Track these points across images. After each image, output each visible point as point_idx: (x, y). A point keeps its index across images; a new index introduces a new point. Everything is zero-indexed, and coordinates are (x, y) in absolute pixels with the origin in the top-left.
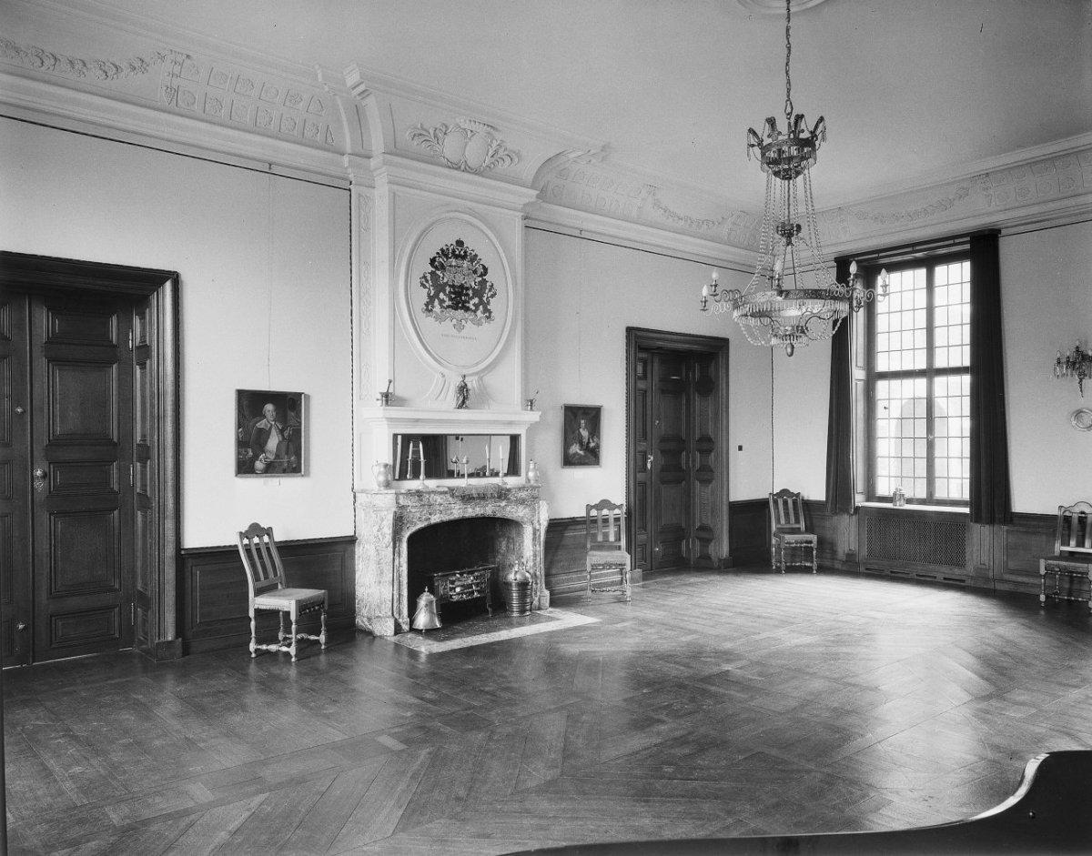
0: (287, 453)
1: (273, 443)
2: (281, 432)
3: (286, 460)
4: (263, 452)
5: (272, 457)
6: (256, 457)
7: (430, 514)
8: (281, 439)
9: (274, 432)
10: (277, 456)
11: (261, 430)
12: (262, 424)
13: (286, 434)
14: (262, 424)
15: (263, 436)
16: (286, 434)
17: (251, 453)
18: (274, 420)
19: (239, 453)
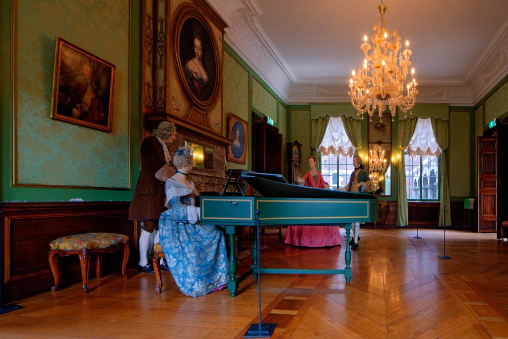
2: (96, 91)
6: (73, 105)
9: (89, 88)
10: (91, 108)
17: (69, 100)
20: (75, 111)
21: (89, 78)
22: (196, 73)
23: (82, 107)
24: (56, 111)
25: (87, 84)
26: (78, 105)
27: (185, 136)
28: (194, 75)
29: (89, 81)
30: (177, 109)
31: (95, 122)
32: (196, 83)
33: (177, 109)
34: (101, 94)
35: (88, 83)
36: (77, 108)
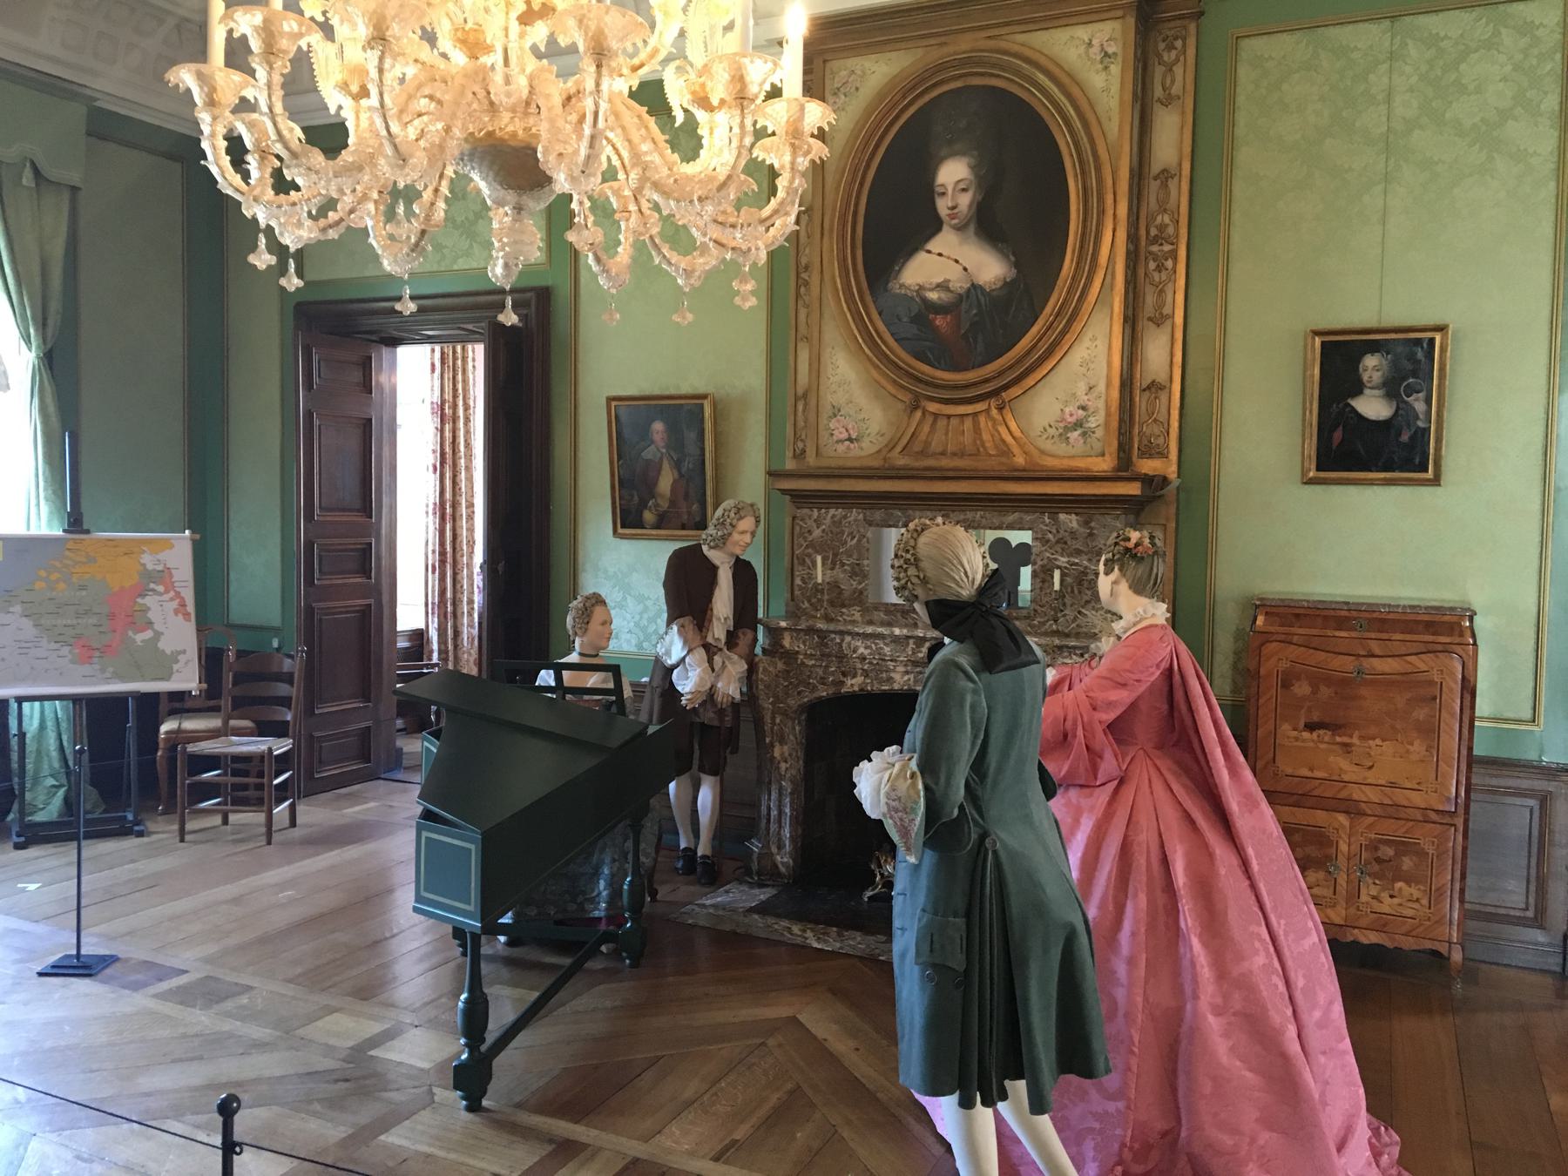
2: (677, 465)
4: (653, 497)
5: (664, 505)
6: (643, 505)
7: (844, 674)
9: (666, 466)
10: (673, 503)
14: (649, 454)
16: (684, 470)
17: (636, 498)
18: (667, 447)
20: (648, 516)
22: (943, 286)
23: (657, 505)
24: (619, 526)
25: (661, 459)
27: (868, 513)
28: (933, 296)
29: (664, 451)
30: (850, 439)
31: (683, 527)
32: (939, 321)
33: (850, 439)
35: (662, 454)
36: (650, 510)
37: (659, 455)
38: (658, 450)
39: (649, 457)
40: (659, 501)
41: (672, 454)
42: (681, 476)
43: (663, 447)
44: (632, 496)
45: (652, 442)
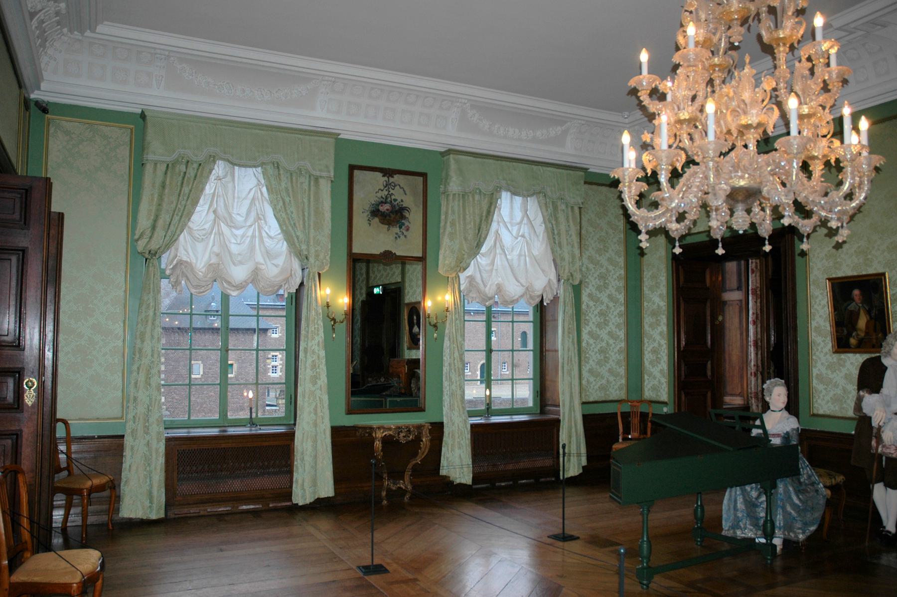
0: (875, 331)
1: (862, 322)
2: (869, 312)
3: (874, 337)
5: (862, 335)
6: (850, 335)
8: (868, 318)
9: (862, 312)
10: (867, 333)
11: (852, 312)
12: (852, 307)
13: (873, 315)
14: (852, 307)
15: (855, 316)
16: (873, 315)
17: (845, 331)
18: (861, 303)
19: (837, 332)
20: (853, 341)
21: (859, 302)
23: (858, 335)
25: (859, 310)
26: (854, 334)
29: (861, 305)
34: (875, 314)
35: (859, 307)
36: (854, 338)
37: (858, 307)
38: (856, 304)
39: (852, 309)
40: (859, 333)
41: (865, 305)
42: (871, 318)
43: (860, 303)
44: (843, 331)
45: (853, 300)
